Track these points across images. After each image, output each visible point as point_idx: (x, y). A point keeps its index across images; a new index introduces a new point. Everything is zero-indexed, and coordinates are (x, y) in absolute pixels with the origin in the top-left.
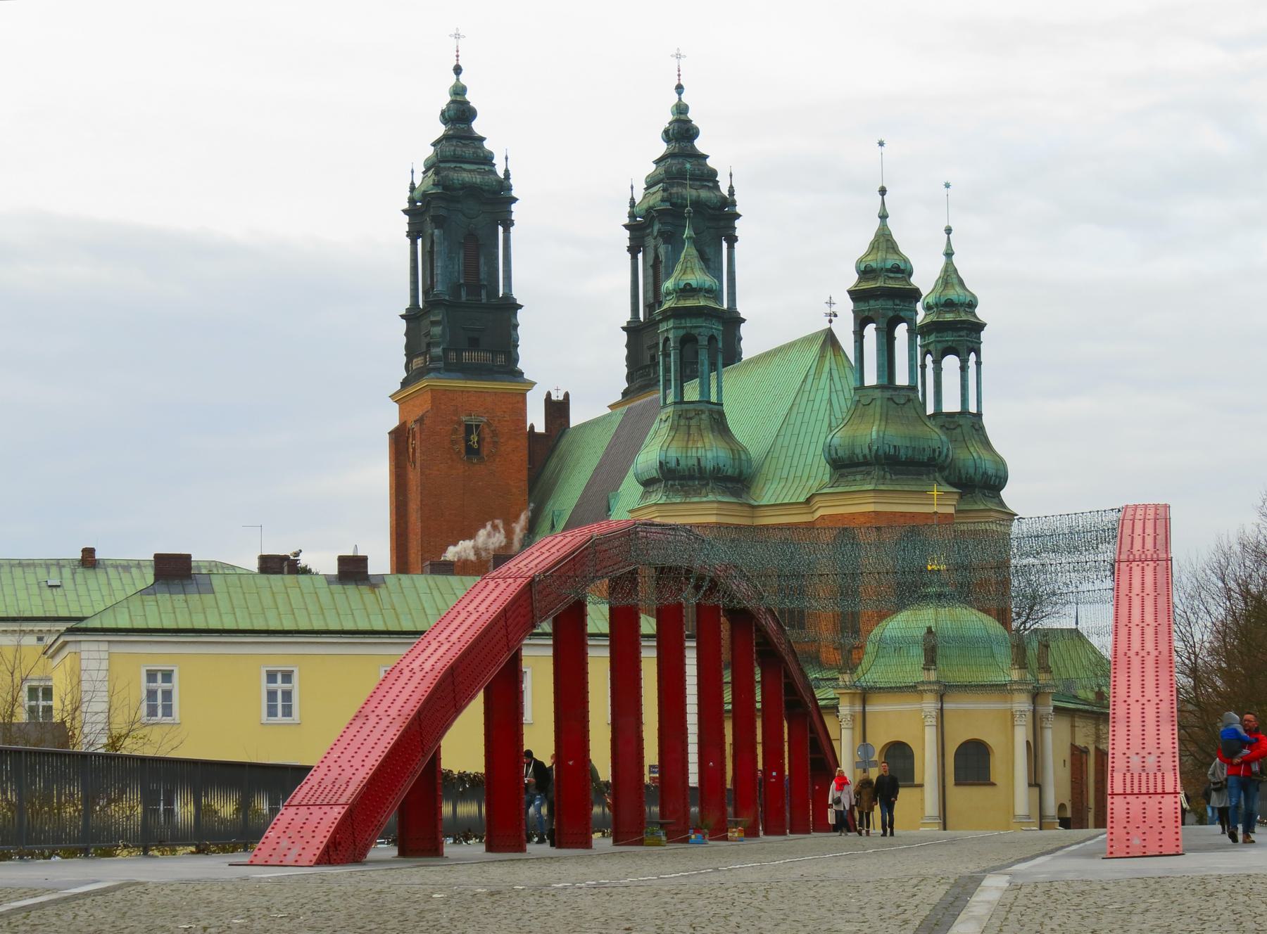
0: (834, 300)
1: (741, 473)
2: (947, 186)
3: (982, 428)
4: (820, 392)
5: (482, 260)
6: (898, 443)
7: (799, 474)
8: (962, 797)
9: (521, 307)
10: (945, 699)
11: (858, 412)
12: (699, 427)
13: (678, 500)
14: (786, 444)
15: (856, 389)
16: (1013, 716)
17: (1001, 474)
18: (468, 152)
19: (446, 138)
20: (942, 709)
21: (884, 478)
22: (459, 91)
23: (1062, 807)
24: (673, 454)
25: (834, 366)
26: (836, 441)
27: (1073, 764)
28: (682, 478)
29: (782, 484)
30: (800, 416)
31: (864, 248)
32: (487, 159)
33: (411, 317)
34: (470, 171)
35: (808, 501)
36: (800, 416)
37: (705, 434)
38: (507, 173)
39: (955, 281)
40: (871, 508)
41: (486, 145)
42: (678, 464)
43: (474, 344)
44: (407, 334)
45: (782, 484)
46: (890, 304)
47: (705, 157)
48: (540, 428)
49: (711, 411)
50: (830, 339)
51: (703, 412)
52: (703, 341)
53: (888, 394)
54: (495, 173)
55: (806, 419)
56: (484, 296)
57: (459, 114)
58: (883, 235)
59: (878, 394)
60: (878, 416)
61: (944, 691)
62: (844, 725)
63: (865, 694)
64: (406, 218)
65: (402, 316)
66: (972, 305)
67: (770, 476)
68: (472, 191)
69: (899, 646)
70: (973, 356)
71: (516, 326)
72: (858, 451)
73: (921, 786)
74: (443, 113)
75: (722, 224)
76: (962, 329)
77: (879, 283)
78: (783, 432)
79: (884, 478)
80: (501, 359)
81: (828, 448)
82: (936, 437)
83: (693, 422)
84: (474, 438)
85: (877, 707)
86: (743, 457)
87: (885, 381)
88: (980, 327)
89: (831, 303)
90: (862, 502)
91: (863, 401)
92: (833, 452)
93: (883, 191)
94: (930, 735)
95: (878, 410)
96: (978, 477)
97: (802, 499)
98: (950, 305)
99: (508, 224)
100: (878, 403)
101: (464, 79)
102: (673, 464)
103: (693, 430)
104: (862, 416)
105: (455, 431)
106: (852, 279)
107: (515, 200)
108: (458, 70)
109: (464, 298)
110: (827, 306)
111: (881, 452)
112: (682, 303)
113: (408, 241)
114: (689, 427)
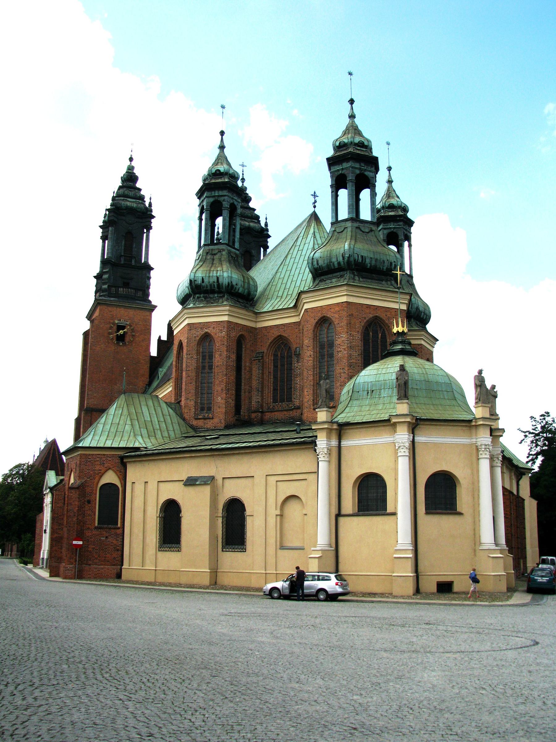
0: (317, 194)
1: (249, 293)
2: (388, 144)
3: (412, 285)
4: (307, 245)
5: (134, 246)
6: (365, 254)
7: (290, 293)
8: (432, 524)
9: (152, 269)
10: (416, 432)
11: (334, 238)
12: (220, 260)
14: (282, 276)
16: (477, 450)
17: (427, 312)
18: (131, 194)
19: (120, 188)
20: (413, 442)
21: (354, 279)
22: (131, 169)
24: (200, 275)
25: (316, 230)
26: (317, 255)
29: (278, 300)
30: (292, 260)
31: (339, 134)
32: (142, 198)
33: (98, 277)
34: (131, 202)
35: (295, 306)
37: (224, 263)
38: (150, 205)
39: (394, 195)
40: (344, 299)
41: (142, 193)
43: (126, 285)
44: (96, 286)
45: (278, 300)
46: (357, 165)
47: (254, 210)
48: (164, 338)
49: (229, 253)
50: (314, 217)
51: (223, 250)
52: (226, 205)
53: (356, 224)
54: (145, 205)
55: (297, 260)
56: (133, 262)
57: (130, 179)
58: (352, 126)
59: (349, 224)
60: (349, 237)
61: (416, 424)
62: (321, 457)
63: (341, 429)
64: (101, 230)
65: (95, 277)
66: (405, 209)
67: (270, 296)
68: (131, 211)
69: (372, 391)
70: (406, 243)
71: (149, 278)
72: (334, 260)
73: (394, 514)
74: (122, 177)
75: (261, 240)
76: (400, 221)
78: (280, 270)
79: (354, 279)
80: (140, 294)
83: (216, 257)
84: (121, 332)
85: (353, 441)
86: (251, 283)
87: (354, 216)
88: (410, 223)
89: (315, 195)
90: (336, 297)
91: (338, 231)
92: (315, 263)
93: (352, 102)
94: (403, 464)
95: (349, 234)
97: (291, 305)
98: (392, 207)
99: (149, 228)
100: (349, 229)
101: (133, 164)
102: (199, 281)
104: (337, 239)
105: (111, 328)
106: (330, 153)
107: (153, 217)
108: (131, 159)
109: (122, 262)
110: (312, 198)
111: (352, 259)
112: (213, 181)
113: (101, 241)
114: (213, 259)
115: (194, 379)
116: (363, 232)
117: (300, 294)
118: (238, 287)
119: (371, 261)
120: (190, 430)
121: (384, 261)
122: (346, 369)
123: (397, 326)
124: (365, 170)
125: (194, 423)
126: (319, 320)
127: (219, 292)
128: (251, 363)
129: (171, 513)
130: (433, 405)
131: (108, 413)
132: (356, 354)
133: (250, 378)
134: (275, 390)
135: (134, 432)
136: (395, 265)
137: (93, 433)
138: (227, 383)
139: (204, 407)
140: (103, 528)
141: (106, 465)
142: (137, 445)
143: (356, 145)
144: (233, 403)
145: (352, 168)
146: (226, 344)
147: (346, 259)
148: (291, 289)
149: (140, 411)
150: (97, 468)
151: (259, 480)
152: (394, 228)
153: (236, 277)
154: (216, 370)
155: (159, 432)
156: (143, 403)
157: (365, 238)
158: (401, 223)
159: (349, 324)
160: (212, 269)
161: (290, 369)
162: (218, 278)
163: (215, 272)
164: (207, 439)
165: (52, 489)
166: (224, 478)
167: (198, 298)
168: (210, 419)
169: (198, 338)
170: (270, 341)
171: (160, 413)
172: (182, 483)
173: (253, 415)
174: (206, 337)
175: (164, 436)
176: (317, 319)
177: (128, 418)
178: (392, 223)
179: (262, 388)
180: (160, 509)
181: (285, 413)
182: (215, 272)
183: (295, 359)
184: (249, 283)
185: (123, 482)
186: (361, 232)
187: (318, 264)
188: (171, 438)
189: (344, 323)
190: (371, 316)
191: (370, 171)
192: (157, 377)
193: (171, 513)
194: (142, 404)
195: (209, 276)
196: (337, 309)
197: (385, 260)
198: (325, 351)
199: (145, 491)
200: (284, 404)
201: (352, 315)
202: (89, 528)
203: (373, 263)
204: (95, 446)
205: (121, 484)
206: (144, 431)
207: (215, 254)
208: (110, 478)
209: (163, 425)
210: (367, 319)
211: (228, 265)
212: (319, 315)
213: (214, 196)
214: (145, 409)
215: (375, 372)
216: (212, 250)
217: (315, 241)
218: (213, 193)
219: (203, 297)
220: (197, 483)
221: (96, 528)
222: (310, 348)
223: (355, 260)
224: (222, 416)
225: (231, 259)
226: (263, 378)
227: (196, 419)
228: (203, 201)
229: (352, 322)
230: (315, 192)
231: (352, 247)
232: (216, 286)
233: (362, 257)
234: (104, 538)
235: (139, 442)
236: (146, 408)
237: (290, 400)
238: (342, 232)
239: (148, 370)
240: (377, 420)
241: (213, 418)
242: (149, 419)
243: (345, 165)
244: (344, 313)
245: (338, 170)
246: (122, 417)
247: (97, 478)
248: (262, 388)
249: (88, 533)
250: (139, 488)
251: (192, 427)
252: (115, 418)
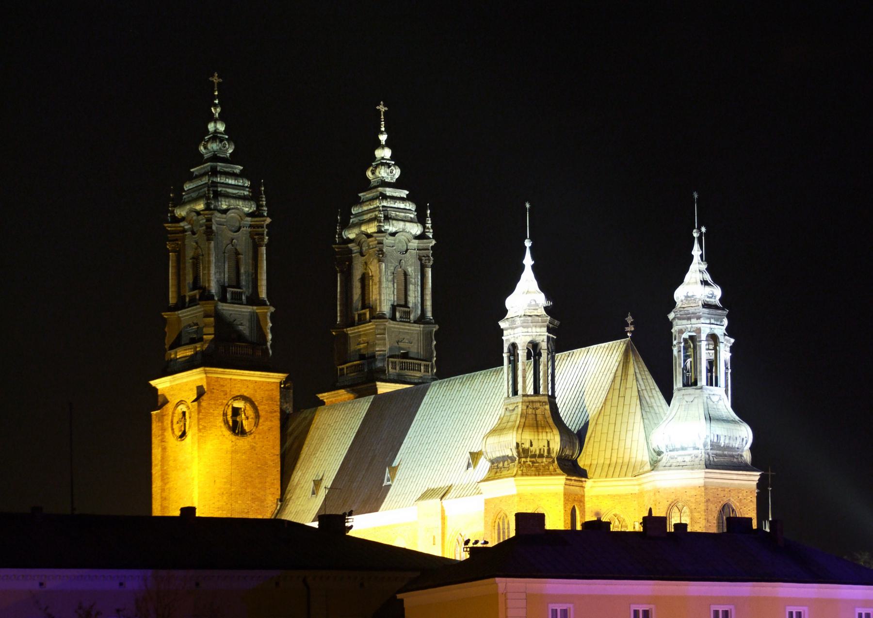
25: (637, 371)
28: (534, 456)
42: (531, 445)
83: (538, 412)
114: (536, 415)
162: (548, 442)
203: (727, 442)
207: (537, 409)
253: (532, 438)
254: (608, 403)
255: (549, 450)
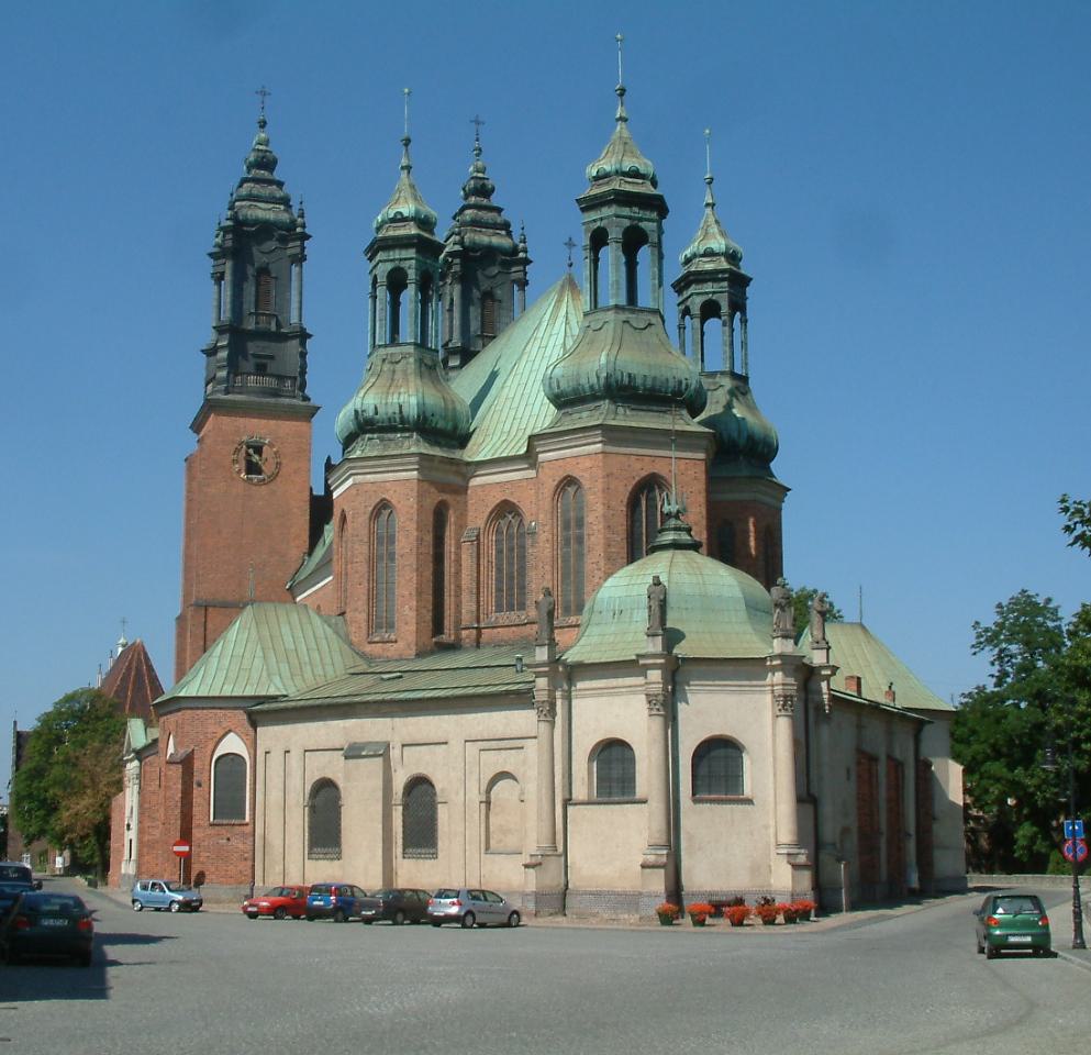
1: (455, 428)
6: (634, 372)
9: (310, 336)
12: (405, 372)
13: (375, 454)
15: (586, 314)
23: (845, 831)
27: (859, 777)
30: (530, 364)
34: (264, 210)
36: (530, 364)
42: (376, 413)
46: (626, 211)
52: (412, 274)
53: (623, 316)
55: (536, 367)
60: (610, 341)
72: (583, 381)
76: (723, 280)
77: (616, 185)
78: (509, 383)
81: (548, 381)
82: (683, 366)
83: (398, 367)
87: (623, 301)
91: (593, 326)
92: (554, 385)
95: (611, 333)
96: (742, 442)
100: (612, 325)
102: (370, 413)
103: (398, 375)
104: (591, 342)
105: (237, 451)
111: (613, 380)
112: (391, 233)
114: (394, 372)
115: (366, 575)
116: (636, 329)
117: (531, 438)
118: (434, 420)
119: (645, 381)
120: (359, 661)
121: (667, 380)
122: (602, 564)
123: (669, 504)
124: (641, 220)
125: (368, 648)
126: (561, 482)
127: (403, 430)
128: (459, 547)
129: (324, 802)
130: (710, 633)
131: (225, 638)
132: (620, 537)
133: (458, 573)
134: (499, 590)
135: (268, 669)
136: (687, 385)
137: (202, 672)
138: (420, 584)
139: (380, 622)
140: (222, 825)
141: (225, 724)
142: (272, 692)
143: (625, 174)
144: (429, 617)
145: (618, 216)
146: (415, 518)
147: (602, 381)
148: (525, 421)
149: (278, 634)
150: (211, 729)
151: (456, 745)
152: (714, 293)
153: (432, 402)
154: (399, 561)
155: (308, 667)
156: (283, 619)
157: (638, 339)
158: (726, 284)
159: (606, 490)
160: (391, 391)
161: (522, 557)
162: (400, 407)
163: (396, 396)
164: (382, 679)
165: (140, 754)
166: (403, 746)
167: (370, 439)
168: (392, 642)
169: (370, 509)
170: (489, 510)
171: (311, 633)
172: (342, 752)
173: (464, 633)
174: (383, 506)
175: (316, 672)
176: (558, 479)
177: (259, 646)
178: (710, 284)
179: (478, 588)
180: (310, 795)
181: (514, 628)
182: (396, 396)
183: (529, 542)
184: (454, 409)
185: (252, 752)
186: (632, 330)
187: (559, 387)
188: (329, 678)
189: (600, 485)
190: (644, 474)
191: (649, 220)
192: (321, 540)
193: (324, 802)
194: (281, 620)
195: (386, 404)
196: (588, 463)
197: (669, 375)
198: (572, 530)
199: (285, 762)
200: (514, 617)
201: (612, 474)
202: (199, 826)
204: (206, 694)
205: (249, 753)
206: (284, 668)
207: (397, 363)
208: (233, 744)
209: (316, 655)
210: (637, 479)
211: (419, 382)
212: (562, 474)
213: (392, 260)
214: (285, 629)
215: (624, 582)
216: (392, 354)
217: (568, 330)
218: (391, 253)
219: (378, 438)
220: (364, 753)
221: (211, 825)
222: (547, 528)
223: (617, 382)
224: (412, 638)
225: (423, 369)
226: (478, 572)
227: (369, 643)
228: (375, 266)
229: (612, 487)
230: (570, 239)
231: (613, 359)
232: (398, 420)
233: (630, 375)
234: (225, 841)
235: (275, 685)
236: (288, 627)
237: (522, 606)
238: (600, 329)
239: (307, 527)
240: (621, 659)
241: (396, 642)
242: (293, 647)
243: (607, 211)
244: (600, 473)
245: (595, 221)
246: (248, 644)
247: (211, 747)
248: (478, 588)
249: (197, 834)
250: (276, 759)
251: (363, 656)
252: (237, 646)
253: (377, 402)
254: (525, 357)
255: (402, 418)
